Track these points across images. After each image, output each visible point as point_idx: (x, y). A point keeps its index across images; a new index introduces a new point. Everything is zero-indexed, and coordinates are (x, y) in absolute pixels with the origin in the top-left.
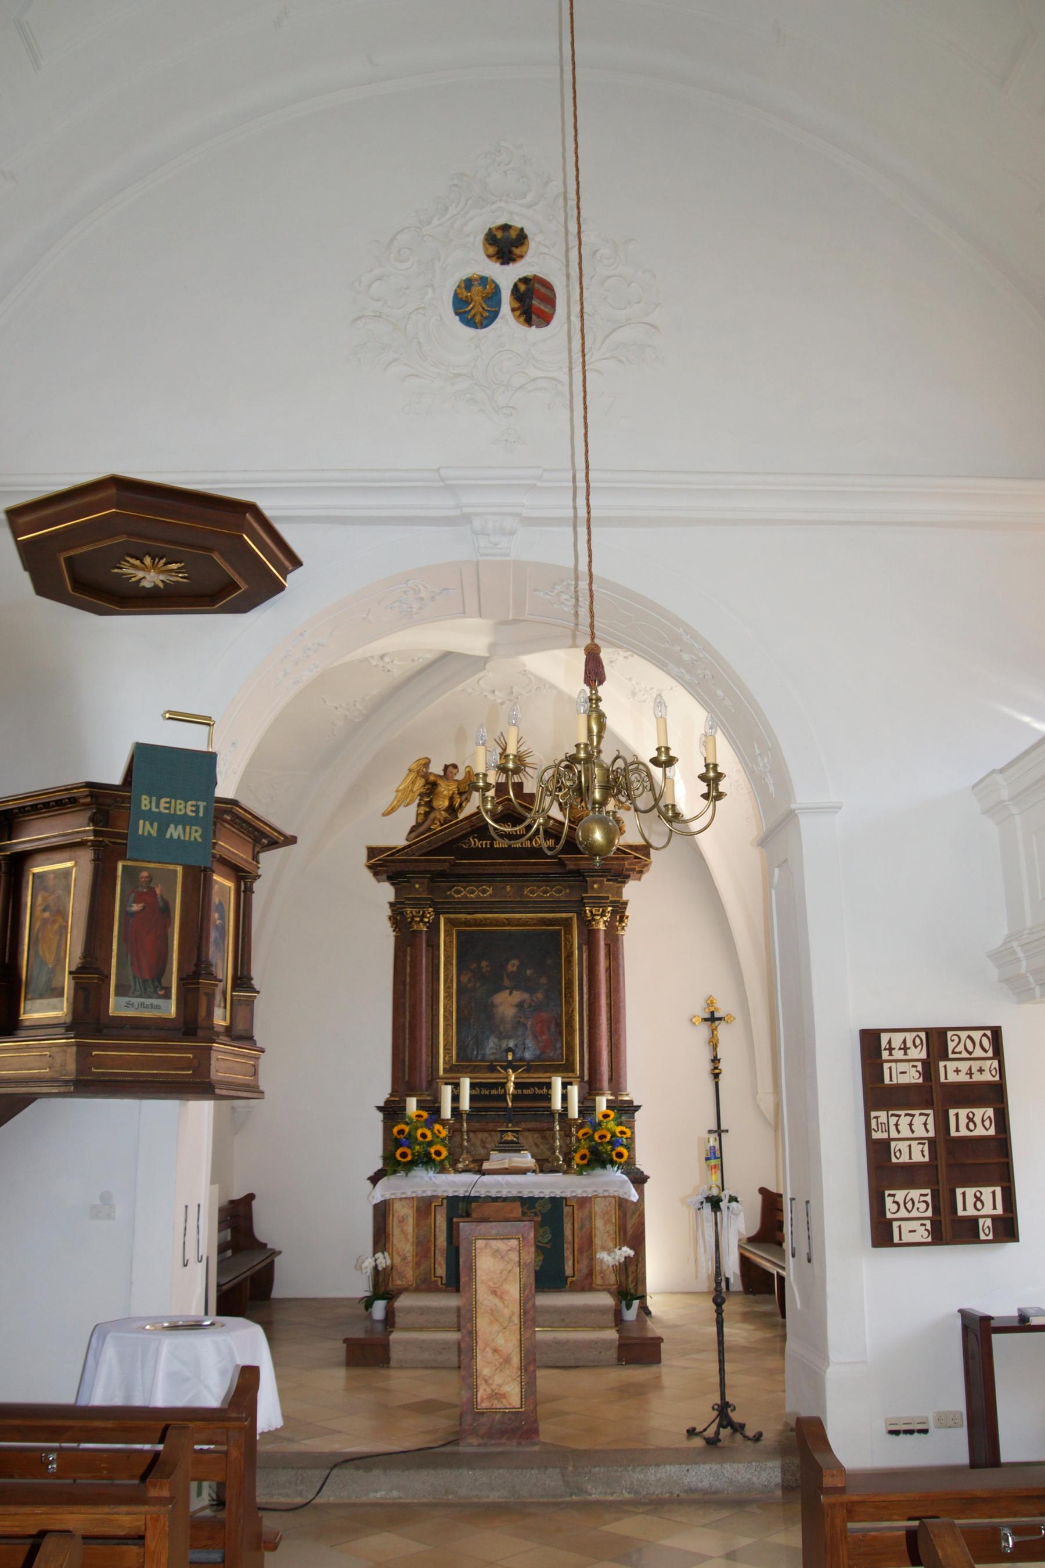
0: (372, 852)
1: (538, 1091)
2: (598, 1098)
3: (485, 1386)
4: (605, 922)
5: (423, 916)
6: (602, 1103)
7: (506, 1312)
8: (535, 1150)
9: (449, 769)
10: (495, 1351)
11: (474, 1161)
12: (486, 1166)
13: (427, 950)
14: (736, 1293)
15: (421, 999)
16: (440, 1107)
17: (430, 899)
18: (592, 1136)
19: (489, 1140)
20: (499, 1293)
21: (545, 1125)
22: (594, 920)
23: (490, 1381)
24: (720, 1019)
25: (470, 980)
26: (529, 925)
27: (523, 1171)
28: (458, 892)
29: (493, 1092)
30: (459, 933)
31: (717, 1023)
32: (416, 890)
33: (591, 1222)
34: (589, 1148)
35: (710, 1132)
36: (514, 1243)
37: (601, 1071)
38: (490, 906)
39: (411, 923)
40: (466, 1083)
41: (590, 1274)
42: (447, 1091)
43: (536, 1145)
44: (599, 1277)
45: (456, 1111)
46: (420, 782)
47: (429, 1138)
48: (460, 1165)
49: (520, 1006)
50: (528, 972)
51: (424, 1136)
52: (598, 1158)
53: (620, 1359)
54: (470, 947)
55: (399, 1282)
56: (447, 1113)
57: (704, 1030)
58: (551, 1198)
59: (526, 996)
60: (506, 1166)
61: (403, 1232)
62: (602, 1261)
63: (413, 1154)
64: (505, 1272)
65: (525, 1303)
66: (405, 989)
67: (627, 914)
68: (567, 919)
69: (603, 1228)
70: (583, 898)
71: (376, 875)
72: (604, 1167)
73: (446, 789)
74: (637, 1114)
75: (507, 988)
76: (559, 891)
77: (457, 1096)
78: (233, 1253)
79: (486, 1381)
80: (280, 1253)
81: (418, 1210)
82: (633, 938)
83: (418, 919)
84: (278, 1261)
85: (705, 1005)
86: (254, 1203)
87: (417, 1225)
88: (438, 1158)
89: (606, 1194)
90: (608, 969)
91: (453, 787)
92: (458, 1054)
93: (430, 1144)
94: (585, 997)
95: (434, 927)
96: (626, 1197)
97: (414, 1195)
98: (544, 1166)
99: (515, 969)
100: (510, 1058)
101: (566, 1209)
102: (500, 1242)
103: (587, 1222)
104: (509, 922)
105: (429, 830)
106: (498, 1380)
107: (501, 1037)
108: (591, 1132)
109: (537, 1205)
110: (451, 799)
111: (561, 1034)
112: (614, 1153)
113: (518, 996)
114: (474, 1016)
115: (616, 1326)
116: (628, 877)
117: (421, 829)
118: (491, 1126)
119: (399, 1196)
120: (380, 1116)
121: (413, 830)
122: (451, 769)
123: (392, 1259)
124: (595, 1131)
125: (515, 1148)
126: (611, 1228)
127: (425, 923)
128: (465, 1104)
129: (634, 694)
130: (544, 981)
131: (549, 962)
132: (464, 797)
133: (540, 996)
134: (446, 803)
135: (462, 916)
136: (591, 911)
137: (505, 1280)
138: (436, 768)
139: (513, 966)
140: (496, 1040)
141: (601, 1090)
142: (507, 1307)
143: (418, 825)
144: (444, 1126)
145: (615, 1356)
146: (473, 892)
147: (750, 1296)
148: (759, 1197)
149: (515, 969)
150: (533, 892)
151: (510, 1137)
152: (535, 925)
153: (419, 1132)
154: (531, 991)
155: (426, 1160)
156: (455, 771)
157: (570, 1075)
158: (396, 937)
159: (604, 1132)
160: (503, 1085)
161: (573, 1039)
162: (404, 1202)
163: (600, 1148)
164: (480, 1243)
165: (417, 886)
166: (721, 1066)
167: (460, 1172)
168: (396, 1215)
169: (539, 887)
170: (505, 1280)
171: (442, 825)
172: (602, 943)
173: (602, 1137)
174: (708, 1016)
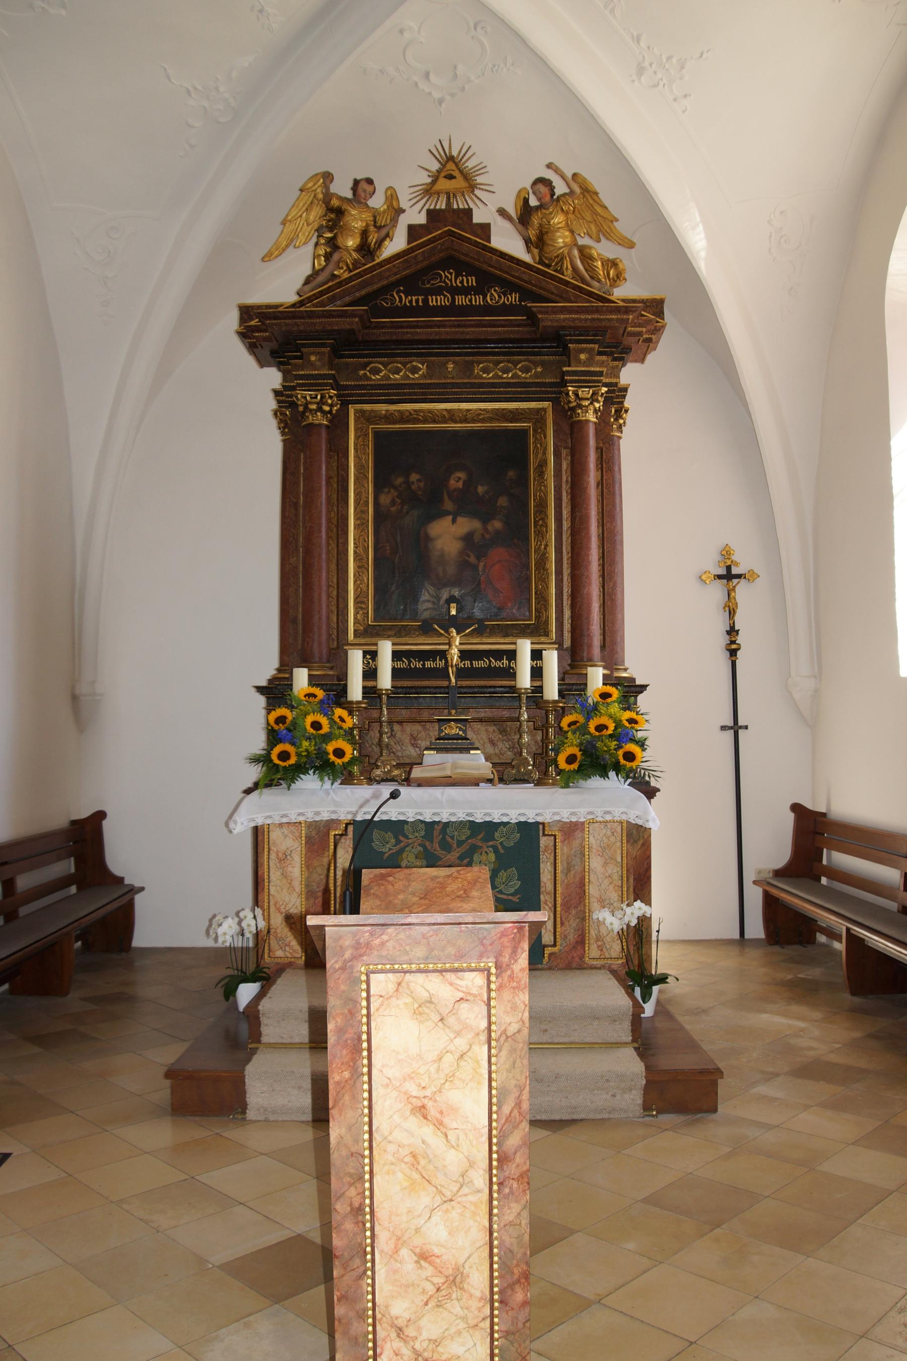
0: (246, 312)
1: (495, 663)
2: (590, 670)
3: (397, 1344)
4: (596, 411)
5: (322, 402)
6: (596, 677)
7: (453, 1160)
8: (490, 749)
9: (362, 187)
10: (424, 1257)
11: (399, 766)
12: (416, 773)
13: (329, 457)
14: (755, 942)
15: (320, 525)
16: (345, 686)
17: (332, 377)
18: (585, 726)
19: (423, 734)
20: (433, 1112)
21: (506, 714)
22: (580, 406)
23: (411, 1332)
24: (739, 576)
25: (393, 503)
26: (483, 421)
27: (474, 782)
28: (376, 371)
29: (428, 664)
30: (377, 435)
31: (735, 581)
32: (313, 366)
33: (583, 861)
34: (580, 745)
35: (723, 728)
36: (474, 981)
37: (590, 635)
38: (423, 393)
39: (304, 412)
40: (386, 648)
41: (581, 941)
42: (356, 660)
43: (492, 743)
44: (594, 947)
45: (370, 692)
46: (317, 212)
47: (326, 729)
48: (378, 772)
49: (468, 539)
50: (481, 490)
51: (316, 725)
52: (595, 762)
53: (647, 1107)
55: (279, 953)
56: (355, 692)
57: (717, 590)
58: (520, 824)
59: (476, 524)
60: (448, 773)
61: (285, 875)
62: (599, 923)
63: (298, 755)
64: (449, 1059)
65: (502, 1137)
66: (297, 515)
67: (626, 405)
68: (538, 411)
69: (603, 873)
70: (564, 374)
71: (252, 348)
72: (604, 775)
73: (356, 220)
74: (640, 698)
75: (448, 513)
76: (526, 370)
77: (372, 665)
78: (79, 889)
79: (400, 1330)
80: (142, 889)
81: (309, 839)
82: (635, 444)
83: (314, 407)
84: (139, 900)
85: (719, 558)
86: (105, 823)
87: (308, 865)
88: (338, 761)
89: (608, 817)
90: (600, 483)
91: (367, 216)
92: (376, 610)
93: (327, 738)
94: (566, 525)
95: (338, 423)
96: (640, 822)
97: (301, 819)
98: (506, 773)
99: (460, 485)
100: (453, 612)
101: (544, 841)
102: (435, 978)
103: (577, 861)
104: (451, 416)
105: (334, 276)
106: (430, 1327)
107: (440, 584)
108: (581, 719)
109: (497, 834)
110: (364, 233)
111: (529, 579)
112: (620, 753)
113: (465, 525)
114: (402, 568)
115: (634, 1041)
116: (627, 350)
117: (321, 278)
118: (425, 715)
119: (277, 820)
120: (262, 700)
121: (308, 281)
122: (364, 185)
123: (268, 919)
124: (588, 718)
125: (462, 745)
126: (615, 871)
127: (323, 412)
128: (385, 681)
129: (641, 70)
130: (503, 501)
131: (511, 474)
132: (383, 232)
133: (497, 525)
134: (358, 240)
135: (383, 408)
136: (577, 395)
137: (450, 1078)
138: (342, 188)
140: (431, 589)
141: (590, 660)
142: (456, 1147)
143: (315, 273)
144: (351, 713)
145: (640, 1101)
146: (397, 371)
147: (777, 948)
148: (791, 816)
150: (487, 372)
151: (453, 730)
152: (491, 420)
153: (310, 719)
154: (485, 520)
155: (323, 766)
156: (369, 188)
157: (543, 639)
158: (284, 441)
159: (604, 720)
160: (443, 654)
161: (547, 587)
162: (285, 830)
163: (599, 744)
164: (381, 983)
165: (313, 358)
166: (740, 639)
167: (379, 782)
168: (274, 849)
169: (497, 363)
170: (450, 1078)
171: (351, 271)
172: (592, 442)
173: (601, 728)
174: (722, 571)
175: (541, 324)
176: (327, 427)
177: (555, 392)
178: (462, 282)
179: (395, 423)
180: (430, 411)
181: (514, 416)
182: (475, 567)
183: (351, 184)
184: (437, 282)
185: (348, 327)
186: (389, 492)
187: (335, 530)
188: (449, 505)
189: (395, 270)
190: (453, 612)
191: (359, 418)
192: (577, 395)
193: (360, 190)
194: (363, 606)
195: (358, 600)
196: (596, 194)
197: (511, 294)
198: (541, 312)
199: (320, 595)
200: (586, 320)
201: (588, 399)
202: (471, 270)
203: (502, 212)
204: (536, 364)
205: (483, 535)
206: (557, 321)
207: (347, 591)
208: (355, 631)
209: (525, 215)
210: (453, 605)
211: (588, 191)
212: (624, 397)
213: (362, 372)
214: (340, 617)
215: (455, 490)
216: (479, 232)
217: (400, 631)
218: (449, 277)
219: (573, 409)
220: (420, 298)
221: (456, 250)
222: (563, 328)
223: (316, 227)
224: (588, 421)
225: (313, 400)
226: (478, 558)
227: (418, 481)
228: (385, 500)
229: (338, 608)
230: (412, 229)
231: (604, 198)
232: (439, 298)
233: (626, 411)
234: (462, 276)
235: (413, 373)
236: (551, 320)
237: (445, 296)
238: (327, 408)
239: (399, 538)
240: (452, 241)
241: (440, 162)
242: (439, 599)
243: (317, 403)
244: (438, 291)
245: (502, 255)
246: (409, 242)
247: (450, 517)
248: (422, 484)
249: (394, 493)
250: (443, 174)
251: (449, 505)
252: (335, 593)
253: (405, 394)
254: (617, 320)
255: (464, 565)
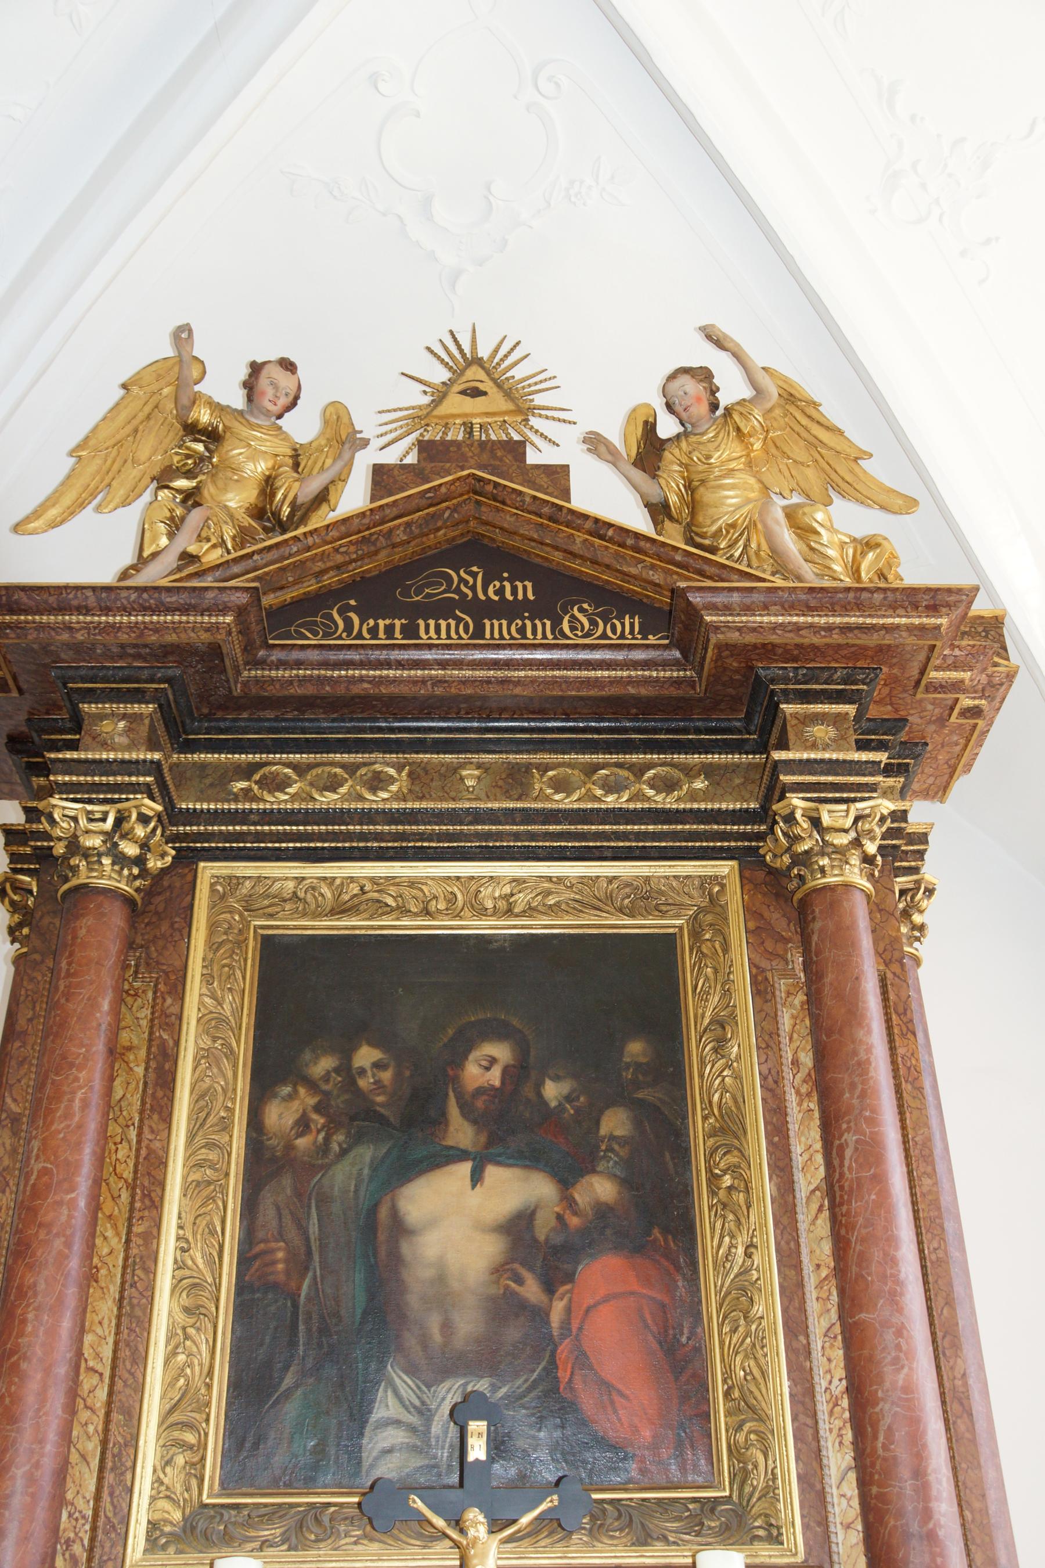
17: (155, 768)
25: (303, 1125)
39: (65, 858)
49: (518, 1228)
50: (552, 1091)
54: (307, 993)
68: (705, 881)
70: (777, 767)
73: (251, 460)
75: (462, 1155)
76: (668, 786)
83: (96, 842)
99: (494, 1077)
100: (477, 1451)
127: (120, 860)
130: (615, 1123)
133: (601, 1188)
139: (486, 1065)
140: (404, 1383)
149: (494, 1077)
154: (566, 1178)
175: (713, 639)
176: (129, 901)
177: (749, 838)
178: (500, 592)
179: (315, 916)
180: (413, 883)
181: (644, 898)
182: (539, 1315)
183: (243, 373)
184: (438, 592)
185: (205, 637)
186: (291, 1097)
187: (125, 1196)
188: (461, 1132)
189: (339, 559)
190: (477, 1451)
191: (223, 897)
192: (816, 822)
193: (263, 382)
194: (190, 1438)
195: (175, 1417)
196: (815, 405)
197: (621, 618)
198: (713, 608)
199: (42, 1397)
200: (829, 628)
201: (846, 831)
202: (519, 566)
203: (595, 443)
204: (690, 772)
205: (559, 1217)
206: (754, 630)
207: (140, 1388)
208: (153, 1526)
209: (650, 452)
210: (477, 1427)
211: (790, 397)
212: (920, 855)
213: (242, 785)
214: (110, 1478)
215: (480, 1091)
216: (543, 480)
217: (301, 1525)
218: (471, 581)
219: (804, 859)
220: (398, 623)
221: (486, 523)
222: (768, 651)
223: (156, 471)
224: (848, 886)
225: (93, 826)
226: (549, 1289)
227: (378, 1065)
228: (280, 1116)
229: (104, 1443)
230: (379, 472)
231: (832, 411)
232: (443, 623)
233: (930, 892)
234: (502, 580)
235: (374, 790)
236: (739, 629)
237: (459, 620)
238: (131, 850)
239: (314, 1229)
240: (478, 502)
241: (450, 369)
242: (425, 1412)
243: (108, 835)
244: (442, 610)
245: (600, 528)
246: (373, 499)
247: (465, 1168)
248: (386, 1076)
249: (307, 1099)
250: (457, 388)
251: (461, 1132)
252: (102, 1394)
253: (349, 836)
254: (910, 629)
255: (504, 1307)
